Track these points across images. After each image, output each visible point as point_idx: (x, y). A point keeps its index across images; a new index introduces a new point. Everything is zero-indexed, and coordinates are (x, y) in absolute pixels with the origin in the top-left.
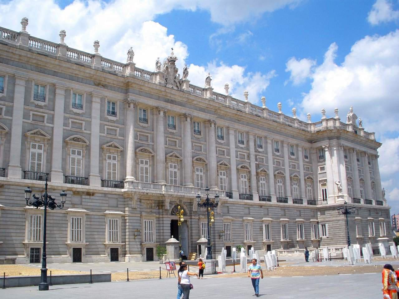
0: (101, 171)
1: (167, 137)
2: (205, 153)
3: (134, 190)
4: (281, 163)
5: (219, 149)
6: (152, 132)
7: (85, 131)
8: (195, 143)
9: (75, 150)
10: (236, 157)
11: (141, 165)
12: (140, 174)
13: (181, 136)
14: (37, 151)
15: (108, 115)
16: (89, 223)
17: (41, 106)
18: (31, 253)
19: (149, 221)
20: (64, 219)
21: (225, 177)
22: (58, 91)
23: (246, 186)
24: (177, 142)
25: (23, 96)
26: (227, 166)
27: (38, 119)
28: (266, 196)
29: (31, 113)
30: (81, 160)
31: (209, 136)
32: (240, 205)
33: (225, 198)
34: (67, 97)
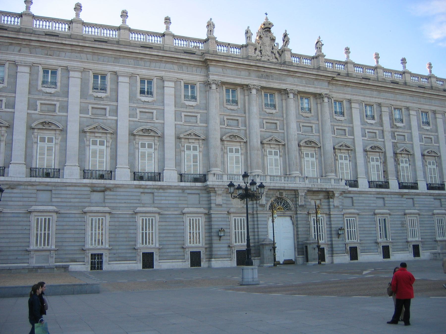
0: (178, 163)
3: (217, 183)
4: (433, 139)
5: (338, 127)
7: (157, 121)
8: (303, 122)
9: (145, 143)
10: (363, 136)
11: (230, 154)
14: (98, 147)
15: (186, 100)
16: (164, 224)
17: (101, 98)
18: (91, 259)
19: (239, 218)
20: (131, 220)
21: (347, 162)
22: (121, 79)
23: (378, 171)
24: (278, 124)
25: (79, 89)
26: (349, 147)
28: (410, 183)
30: (153, 154)
32: (370, 195)
33: (342, 187)
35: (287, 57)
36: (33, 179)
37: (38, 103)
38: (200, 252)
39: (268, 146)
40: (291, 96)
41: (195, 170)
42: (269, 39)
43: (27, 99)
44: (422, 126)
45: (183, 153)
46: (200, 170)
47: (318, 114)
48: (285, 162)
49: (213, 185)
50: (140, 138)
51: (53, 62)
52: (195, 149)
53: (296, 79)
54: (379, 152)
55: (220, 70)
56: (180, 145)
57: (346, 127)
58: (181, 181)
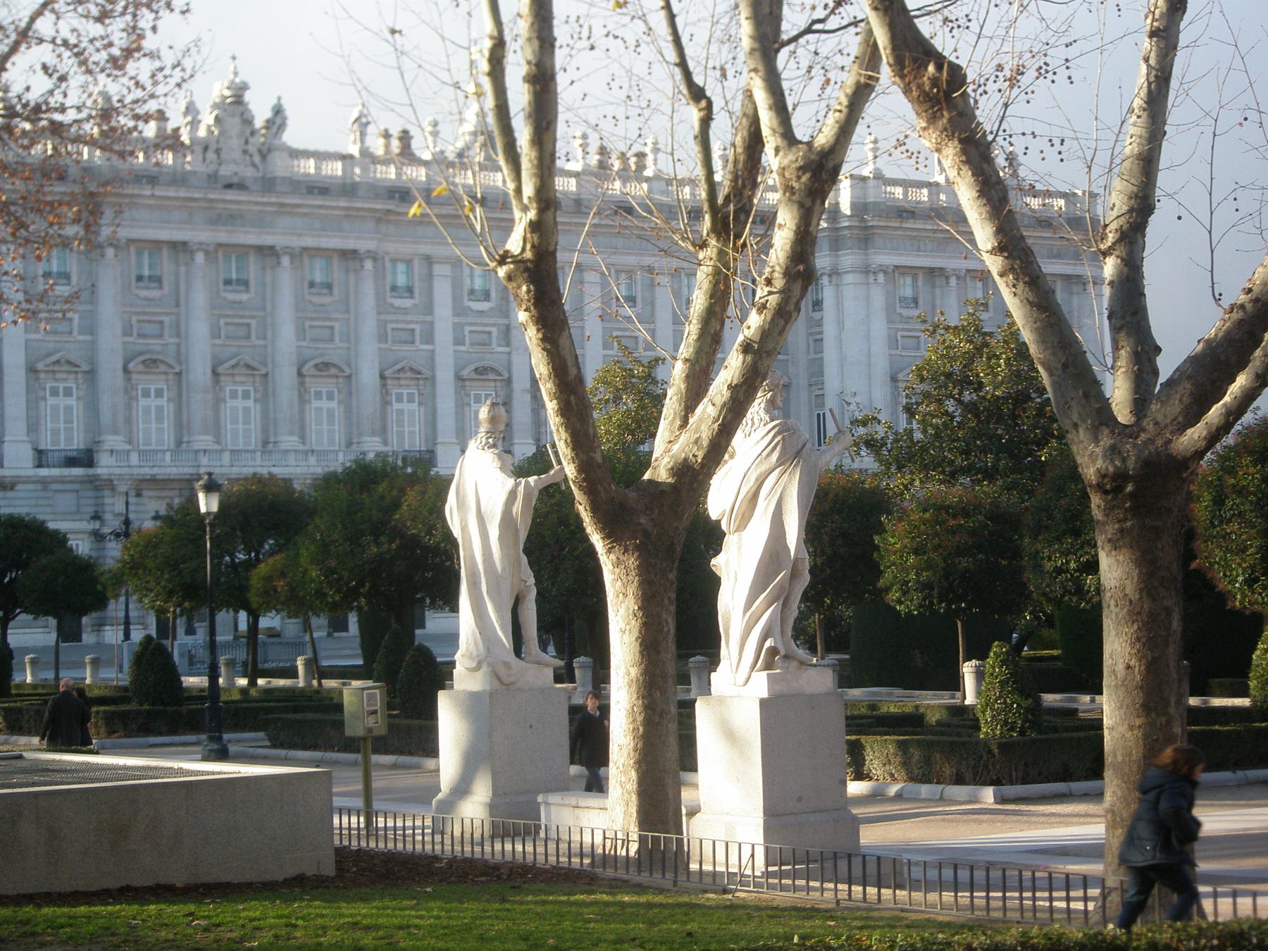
0: (33, 427)
2: (345, 345)
3: (118, 471)
5: (395, 326)
8: (312, 319)
11: (143, 402)
13: (264, 308)
21: (415, 406)
26: (419, 373)
35: (279, 166)
41: (69, 439)
42: (237, 120)
45: (42, 403)
46: (77, 442)
48: (265, 414)
49: (110, 475)
54: (495, 380)
56: (37, 385)
57: (417, 323)
58: (40, 466)
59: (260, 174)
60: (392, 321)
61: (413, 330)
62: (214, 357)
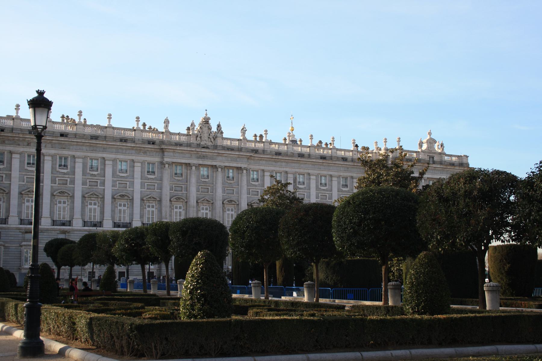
1: (200, 186)
2: (238, 195)
5: (252, 190)
6: (186, 183)
7: (129, 189)
8: (228, 187)
11: (175, 210)
12: (174, 217)
13: (213, 184)
14: (93, 207)
17: (95, 175)
18: (89, 275)
22: (107, 162)
24: (209, 189)
25: (81, 169)
27: (93, 184)
29: (88, 180)
31: (241, 181)
34: (114, 166)
36: (56, 227)
37: (57, 179)
38: (153, 272)
39: (202, 204)
40: (220, 170)
41: (153, 220)
42: (207, 128)
43: (50, 177)
44: (320, 187)
45: (145, 210)
47: (238, 181)
50: (119, 200)
51: (65, 152)
52: (153, 207)
53: (224, 158)
55: (172, 154)
59: (213, 144)
60: (252, 189)
61: (258, 191)
62: (197, 197)
